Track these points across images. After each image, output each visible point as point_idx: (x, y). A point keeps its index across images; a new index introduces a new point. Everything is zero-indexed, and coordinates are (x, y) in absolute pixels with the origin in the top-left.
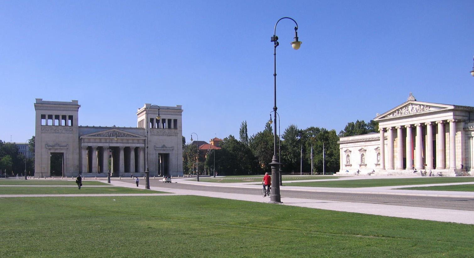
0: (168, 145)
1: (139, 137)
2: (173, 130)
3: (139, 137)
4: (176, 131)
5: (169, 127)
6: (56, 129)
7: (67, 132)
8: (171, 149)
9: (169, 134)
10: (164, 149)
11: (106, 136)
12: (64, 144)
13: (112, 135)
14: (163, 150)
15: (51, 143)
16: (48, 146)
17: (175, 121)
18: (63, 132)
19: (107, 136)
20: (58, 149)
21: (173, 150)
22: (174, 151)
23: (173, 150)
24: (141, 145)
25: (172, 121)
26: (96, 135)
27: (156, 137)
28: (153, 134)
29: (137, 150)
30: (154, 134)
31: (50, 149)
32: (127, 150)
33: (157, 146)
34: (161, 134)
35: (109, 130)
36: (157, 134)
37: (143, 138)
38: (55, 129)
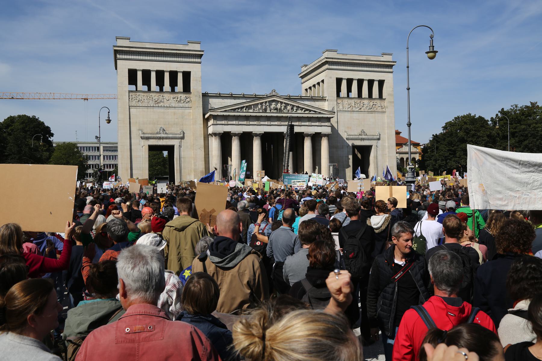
0: (372, 132)
1: (320, 113)
2: (378, 102)
3: (320, 113)
6: (158, 99)
7: (181, 105)
10: (363, 137)
16: (144, 133)
17: (381, 83)
18: (173, 105)
19: (261, 111)
23: (379, 139)
24: (326, 130)
26: (238, 108)
31: (148, 138)
33: (349, 133)
34: (357, 109)
36: (349, 109)
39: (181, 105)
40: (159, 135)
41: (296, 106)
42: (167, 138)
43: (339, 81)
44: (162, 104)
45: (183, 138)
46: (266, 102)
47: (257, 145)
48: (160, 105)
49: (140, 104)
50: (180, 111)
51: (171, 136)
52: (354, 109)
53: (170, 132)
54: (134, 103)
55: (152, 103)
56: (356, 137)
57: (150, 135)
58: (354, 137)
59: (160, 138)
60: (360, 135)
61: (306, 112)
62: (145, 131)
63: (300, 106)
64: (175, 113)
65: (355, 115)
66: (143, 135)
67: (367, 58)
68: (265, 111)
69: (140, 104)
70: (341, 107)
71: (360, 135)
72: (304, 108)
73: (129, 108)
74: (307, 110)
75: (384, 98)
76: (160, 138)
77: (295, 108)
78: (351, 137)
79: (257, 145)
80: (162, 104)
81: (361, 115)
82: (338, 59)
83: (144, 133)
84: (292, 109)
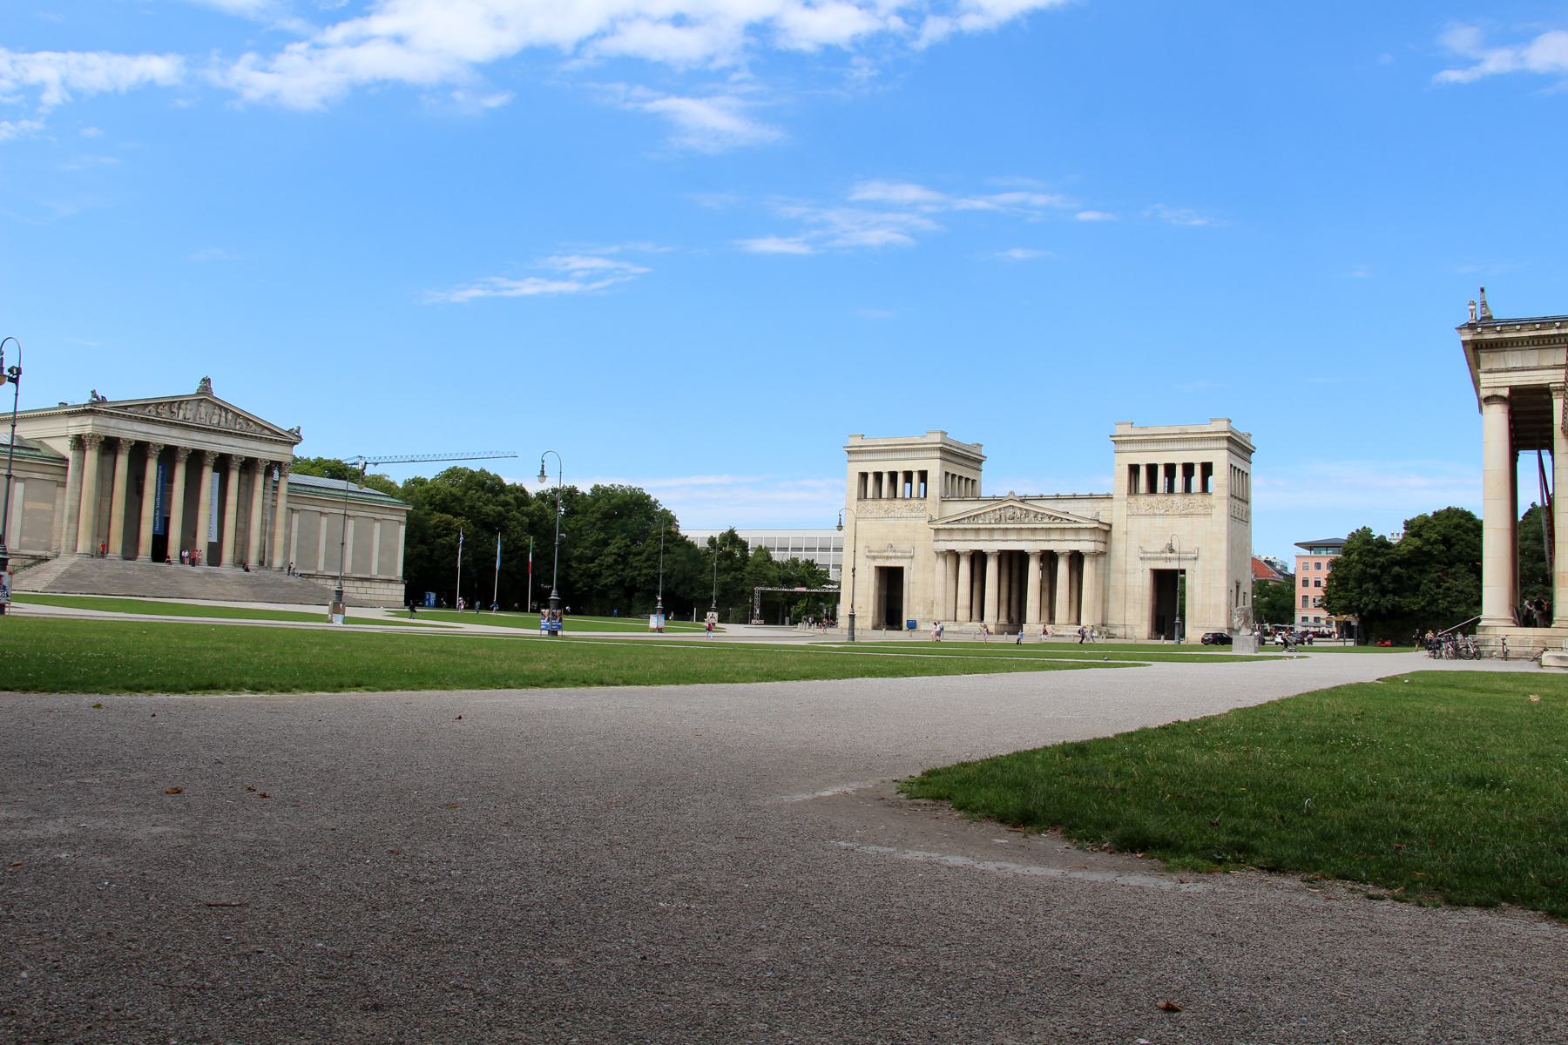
2: (1199, 498)
4: (1206, 499)
5: (1152, 488)
7: (914, 514)
8: (1189, 556)
9: (1183, 512)
11: (990, 523)
12: (905, 546)
13: (1003, 518)
14: (1166, 558)
15: (875, 547)
16: (870, 551)
17: (1207, 469)
18: (905, 515)
20: (891, 557)
21: (1196, 559)
22: (1199, 561)
23: (1196, 559)
24: (1085, 545)
25: (1161, 472)
26: (964, 519)
27: (1145, 521)
28: (1135, 510)
29: (1076, 559)
30: (1140, 513)
31: (874, 558)
32: (1049, 559)
33: (1146, 550)
34: (1162, 512)
35: (996, 505)
37: (1089, 526)
38: (886, 507)
39: (914, 514)
40: (885, 554)
41: (1042, 514)
42: (895, 557)
43: (1134, 469)
44: (892, 514)
45: (912, 557)
46: (1000, 509)
47: (992, 568)
48: (890, 515)
49: (869, 515)
50: (913, 522)
51: (899, 554)
52: (1157, 512)
53: (900, 549)
54: (861, 515)
55: (882, 514)
56: (1158, 555)
57: (876, 554)
58: (1152, 555)
59: (887, 558)
60: (1162, 552)
61: (1056, 521)
62: (872, 549)
63: (1047, 513)
64: (906, 526)
65: (1158, 521)
66: (868, 554)
67: (1181, 429)
68: (999, 521)
69: (869, 515)
70: (1135, 510)
71: (1162, 552)
72: (1052, 516)
73: (856, 521)
74: (1056, 518)
75: (1209, 491)
76: (887, 558)
77: (1040, 516)
78: (1149, 555)
79: (992, 568)
80: (892, 514)
81: (1168, 521)
82: (1130, 436)
83: (870, 551)
84: (1035, 517)
